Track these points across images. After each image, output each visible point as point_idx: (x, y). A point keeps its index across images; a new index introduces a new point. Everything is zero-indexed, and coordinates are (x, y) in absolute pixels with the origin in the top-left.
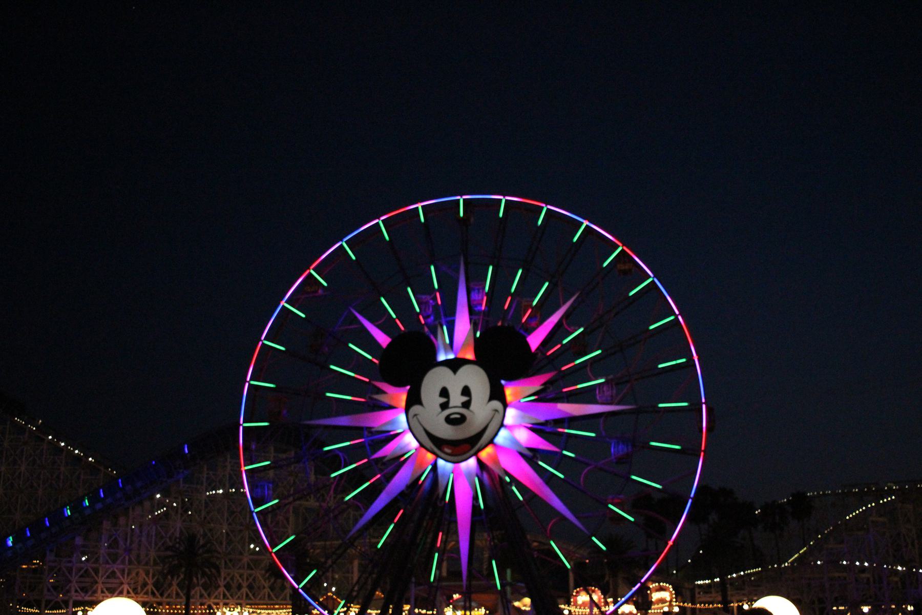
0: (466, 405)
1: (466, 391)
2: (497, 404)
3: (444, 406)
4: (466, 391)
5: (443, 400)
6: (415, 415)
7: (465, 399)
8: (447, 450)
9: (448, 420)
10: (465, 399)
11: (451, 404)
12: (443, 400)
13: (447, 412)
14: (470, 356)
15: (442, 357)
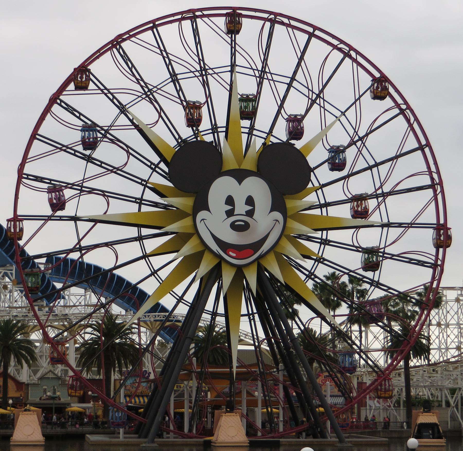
0: (250, 213)
1: (250, 201)
2: (278, 215)
3: (230, 213)
4: (250, 201)
5: (229, 208)
6: (203, 220)
7: (250, 208)
8: (231, 253)
9: (234, 226)
10: (250, 208)
11: (235, 214)
12: (229, 208)
13: (232, 219)
14: (254, 168)
15: (226, 168)
